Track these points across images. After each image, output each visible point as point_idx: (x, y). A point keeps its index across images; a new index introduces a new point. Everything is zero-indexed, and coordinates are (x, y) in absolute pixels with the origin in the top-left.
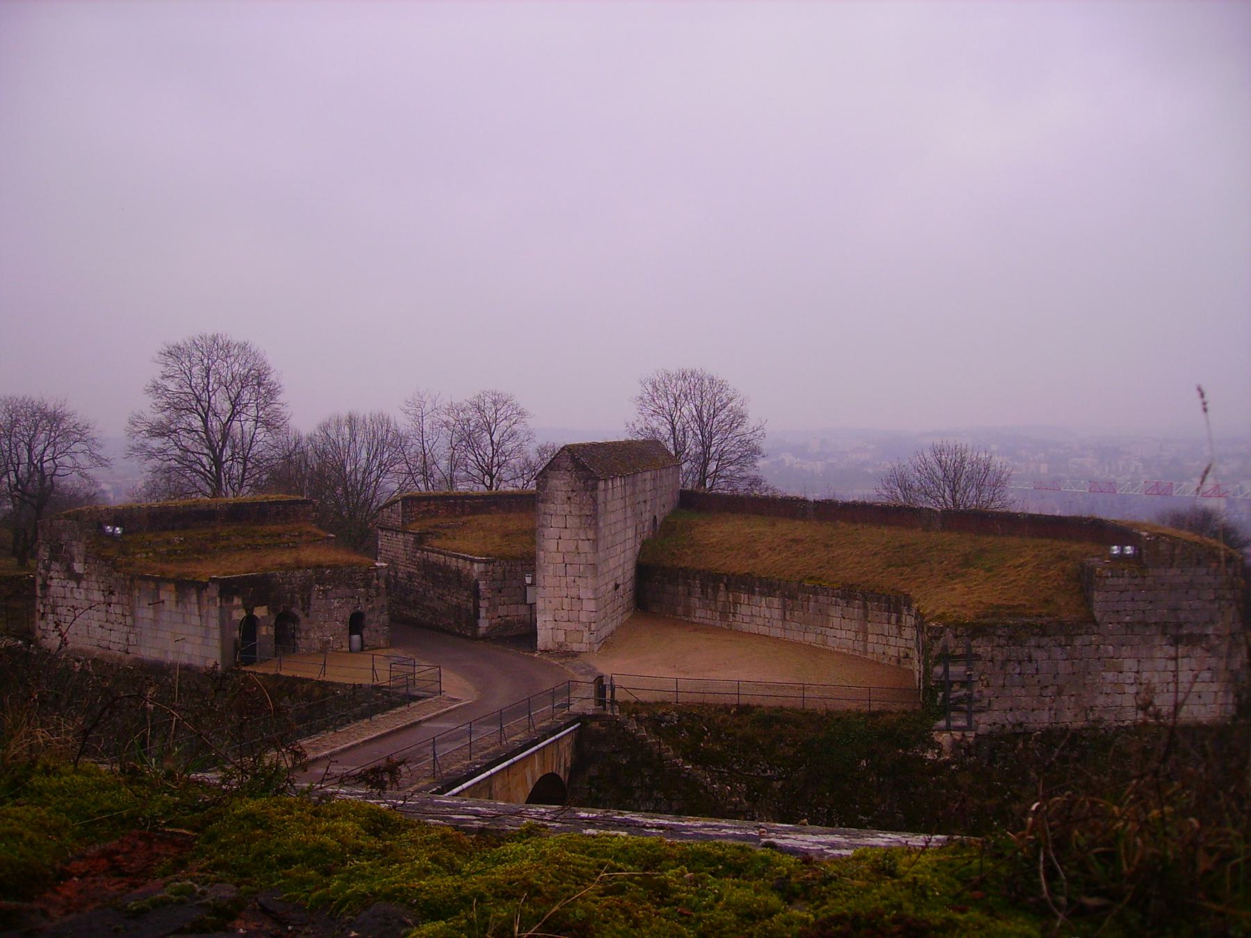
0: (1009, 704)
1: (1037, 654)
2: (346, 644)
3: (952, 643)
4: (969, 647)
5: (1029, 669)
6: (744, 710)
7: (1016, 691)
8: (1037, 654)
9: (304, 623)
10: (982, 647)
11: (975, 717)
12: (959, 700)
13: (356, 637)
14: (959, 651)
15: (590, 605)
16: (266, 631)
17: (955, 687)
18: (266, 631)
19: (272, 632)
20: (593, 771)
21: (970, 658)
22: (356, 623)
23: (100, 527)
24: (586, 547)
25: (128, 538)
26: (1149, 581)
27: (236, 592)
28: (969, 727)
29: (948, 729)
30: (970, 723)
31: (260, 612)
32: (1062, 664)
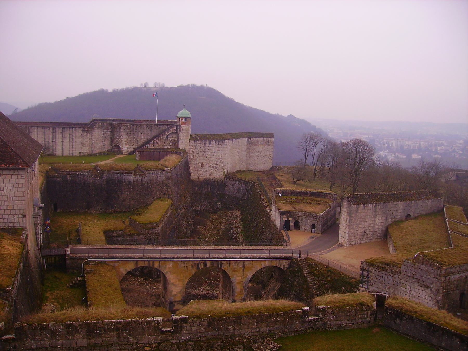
0: (377, 286)
1: (384, 276)
2: (311, 231)
3: (365, 266)
4: (368, 269)
5: (382, 279)
6: (327, 267)
7: (379, 284)
8: (384, 276)
9: (301, 224)
10: (372, 270)
11: (369, 287)
12: (365, 281)
13: (313, 230)
14: (367, 269)
15: (347, 235)
16: (292, 224)
17: (365, 277)
18: (292, 224)
19: (293, 224)
20: (291, 269)
21: (369, 272)
22: (314, 226)
23: (278, 193)
24: (348, 220)
25: (283, 197)
26: (416, 266)
27: (285, 214)
28: (367, 288)
29: (362, 287)
30: (367, 287)
31: (290, 219)
32: (391, 281)
